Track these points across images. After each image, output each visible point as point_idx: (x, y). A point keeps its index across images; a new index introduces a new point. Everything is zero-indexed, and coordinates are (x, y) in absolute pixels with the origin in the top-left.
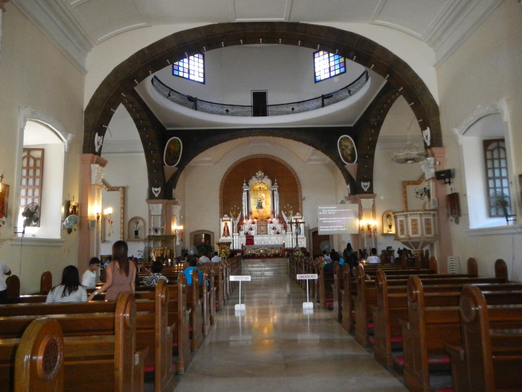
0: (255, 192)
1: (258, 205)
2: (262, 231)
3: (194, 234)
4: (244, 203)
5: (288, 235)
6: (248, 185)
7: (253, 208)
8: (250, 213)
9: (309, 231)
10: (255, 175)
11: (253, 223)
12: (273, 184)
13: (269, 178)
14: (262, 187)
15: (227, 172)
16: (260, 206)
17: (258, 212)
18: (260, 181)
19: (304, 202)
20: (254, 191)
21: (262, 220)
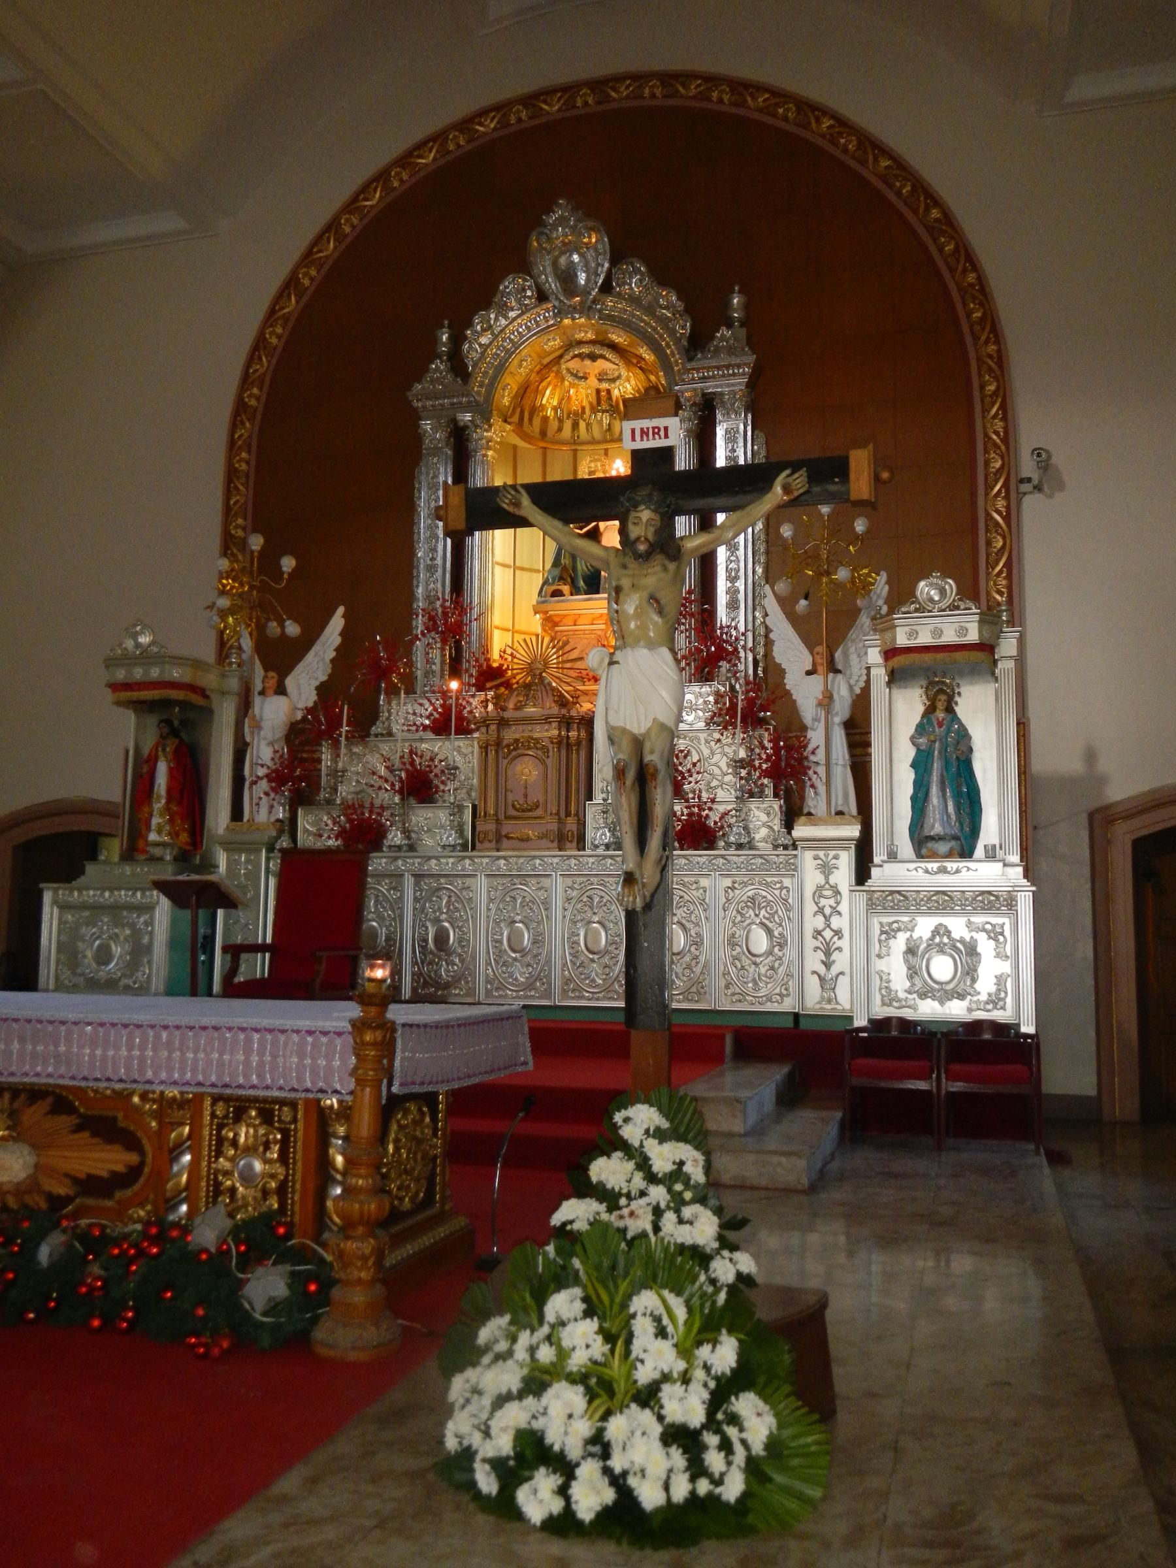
2: (526, 811)
3: (21, 835)
5: (808, 860)
9: (1101, 820)
10: (524, 267)
11: (447, 723)
13: (661, 276)
15: (291, 284)
17: (550, 622)
19: (1032, 505)
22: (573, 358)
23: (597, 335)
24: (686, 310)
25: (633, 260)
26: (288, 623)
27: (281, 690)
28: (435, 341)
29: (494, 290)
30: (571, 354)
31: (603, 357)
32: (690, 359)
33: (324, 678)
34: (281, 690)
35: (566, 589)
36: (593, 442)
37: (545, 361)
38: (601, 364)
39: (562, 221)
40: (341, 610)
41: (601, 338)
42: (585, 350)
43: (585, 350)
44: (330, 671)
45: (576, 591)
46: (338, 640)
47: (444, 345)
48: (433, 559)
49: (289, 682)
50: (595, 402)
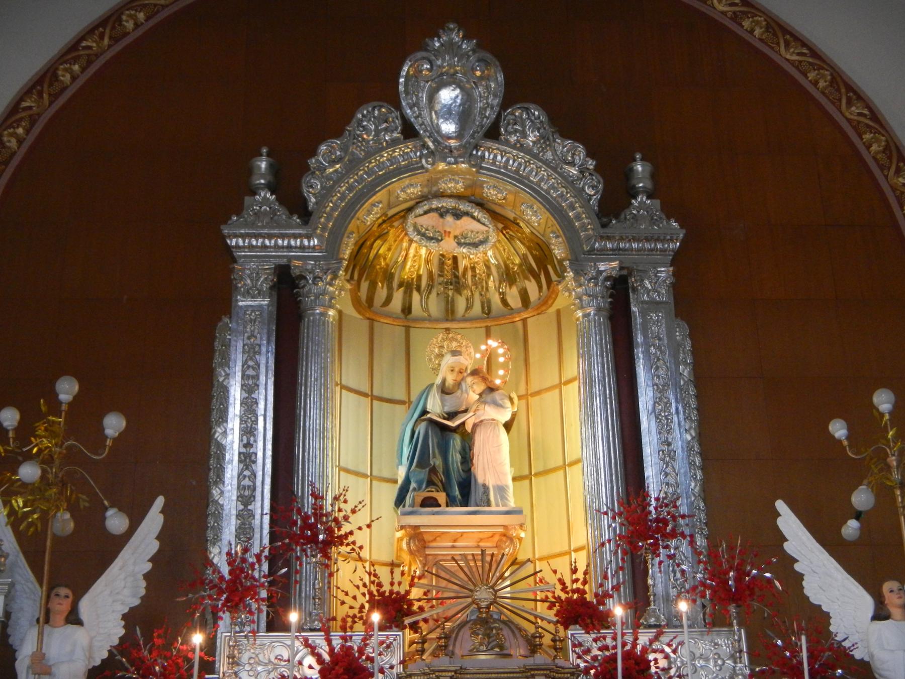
0: (390, 334)
1: (420, 458)
4: (231, 435)
6: (299, 209)
7: (356, 456)
8: (302, 530)
12: (613, 205)
13: (564, 124)
14: (467, 257)
16: (443, 469)
18: (454, 176)
20: (365, 305)
21: (489, 624)
22: (426, 213)
23: (466, 188)
24: (597, 169)
25: (531, 106)
26: (110, 513)
27: (73, 618)
28: (250, 171)
29: (348, 117)
30: (426, 208)
31: (467, 214)
32: (604, 226)
33: (136, 602)
34: (73, 618)
35: (441, 497)
36: (430, 319)
37: (391, 213)
38: (466, 224)
39: (451, 48)
40: (160, 501)
41: (469, 193)
42: (449, 203)
43: (449, 203)
44: (143, 592)
45: (451, 502)
46: (155, 546)
47: (262, 176)
48: (248, 445)
49: (85, 606)
50: (435, 270)
